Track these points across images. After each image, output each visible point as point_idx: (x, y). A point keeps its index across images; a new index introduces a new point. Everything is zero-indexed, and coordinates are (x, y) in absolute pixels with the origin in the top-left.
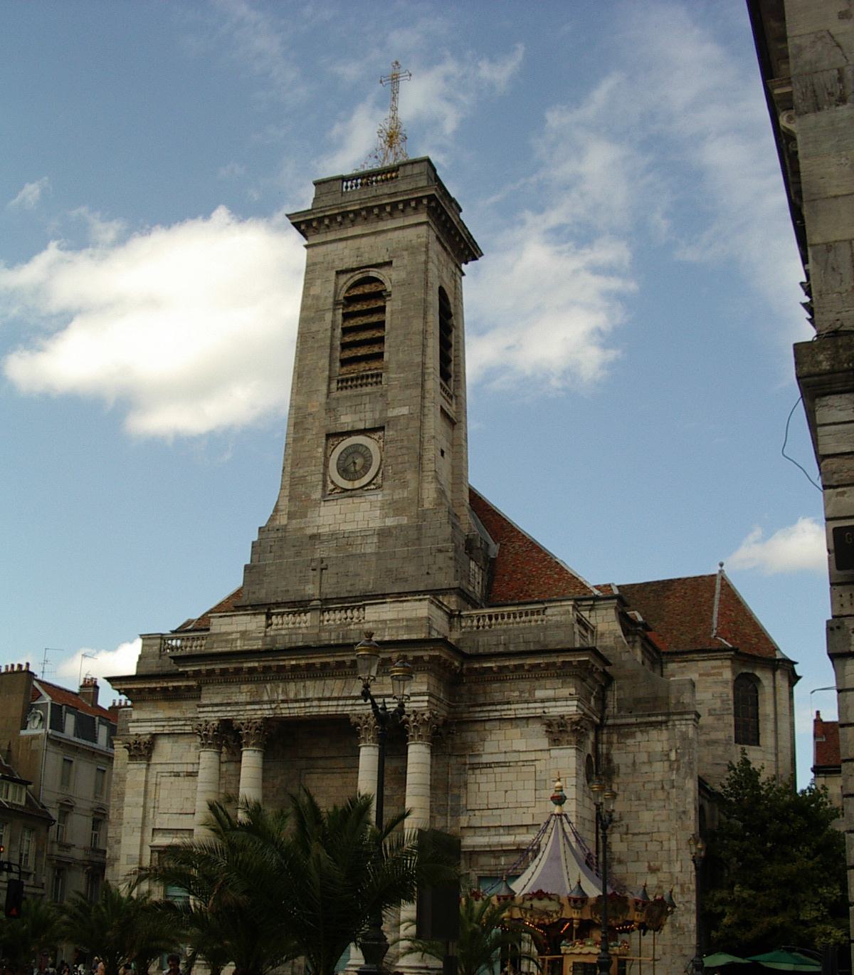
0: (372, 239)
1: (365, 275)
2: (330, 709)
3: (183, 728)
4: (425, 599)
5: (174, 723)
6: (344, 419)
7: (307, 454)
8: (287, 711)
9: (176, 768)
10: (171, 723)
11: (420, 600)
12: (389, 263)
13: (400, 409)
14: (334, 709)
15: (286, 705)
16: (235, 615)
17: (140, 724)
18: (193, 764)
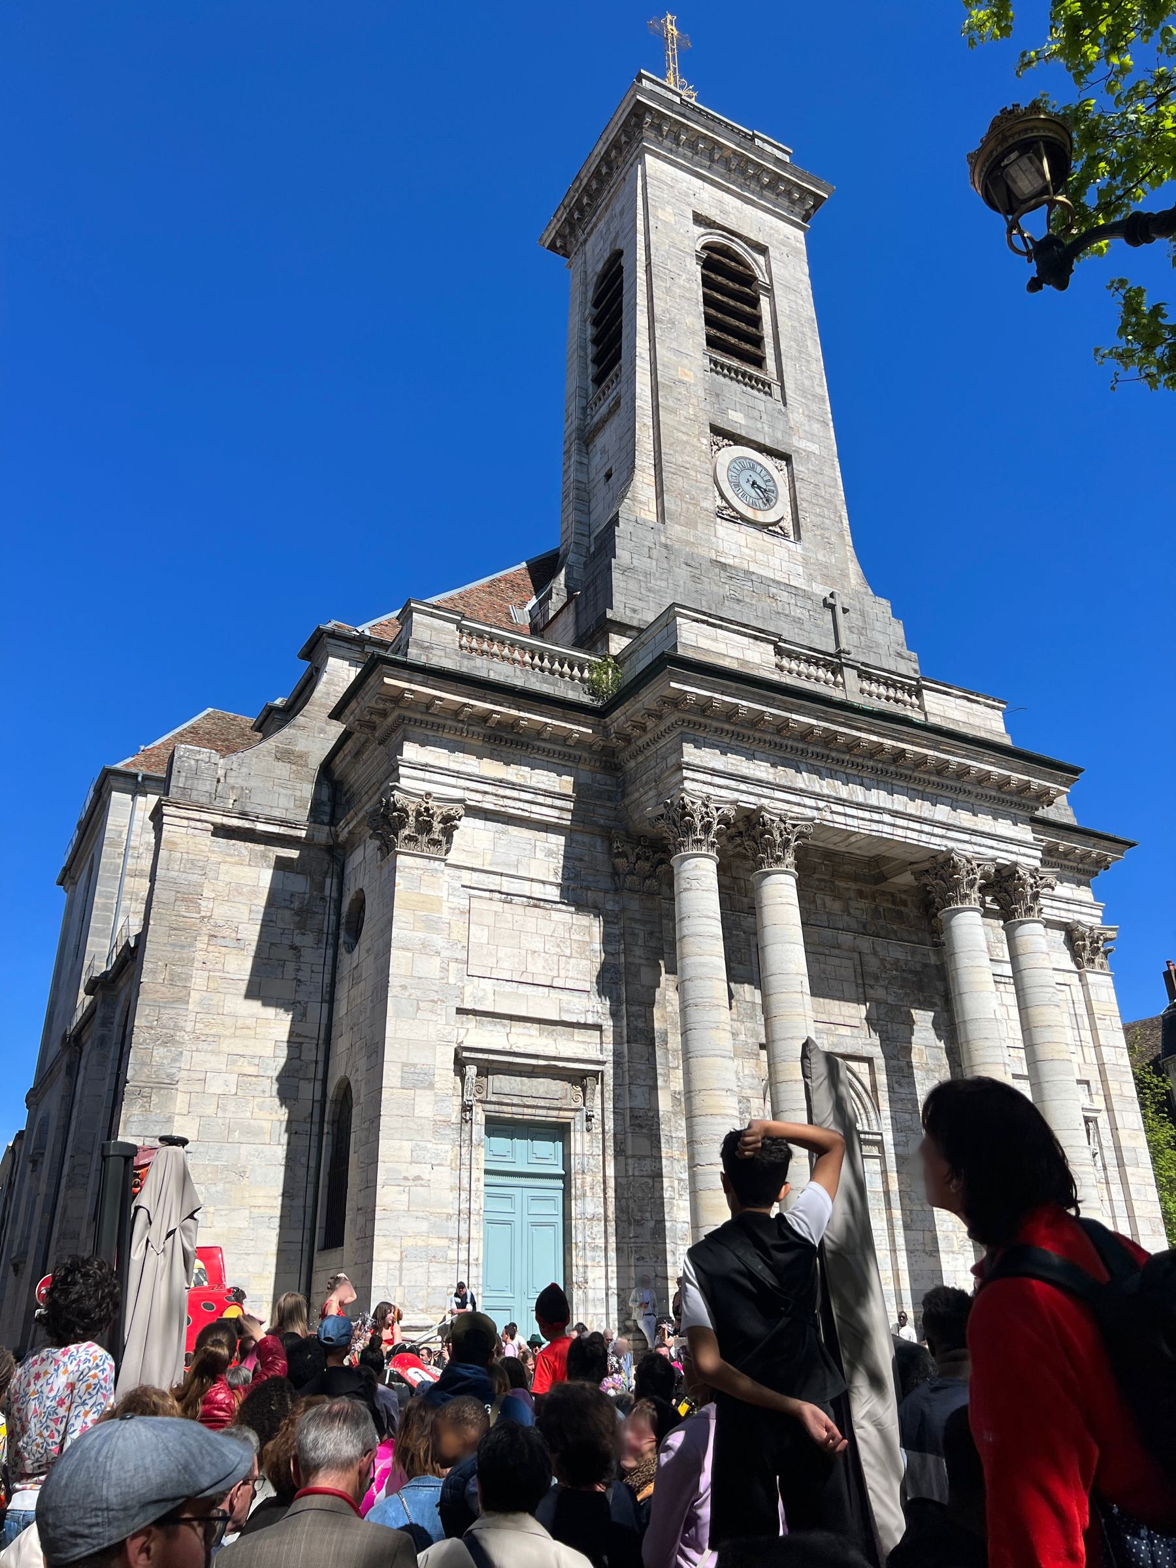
0: (738, 203)
2: (910, 834)
3: (526, 806)
4: (998, 709)
5: (508, 793)
6: (733, 415)
7: (685, 438)
8: (841, 819)
9: (508, 885)
10: (501, 792)
11: (993, 707)
13: (809, 444)
14: (915, 835)
15: (840, 809)
16: (720, 627)
17: (428, 776)
18: (543, 882)
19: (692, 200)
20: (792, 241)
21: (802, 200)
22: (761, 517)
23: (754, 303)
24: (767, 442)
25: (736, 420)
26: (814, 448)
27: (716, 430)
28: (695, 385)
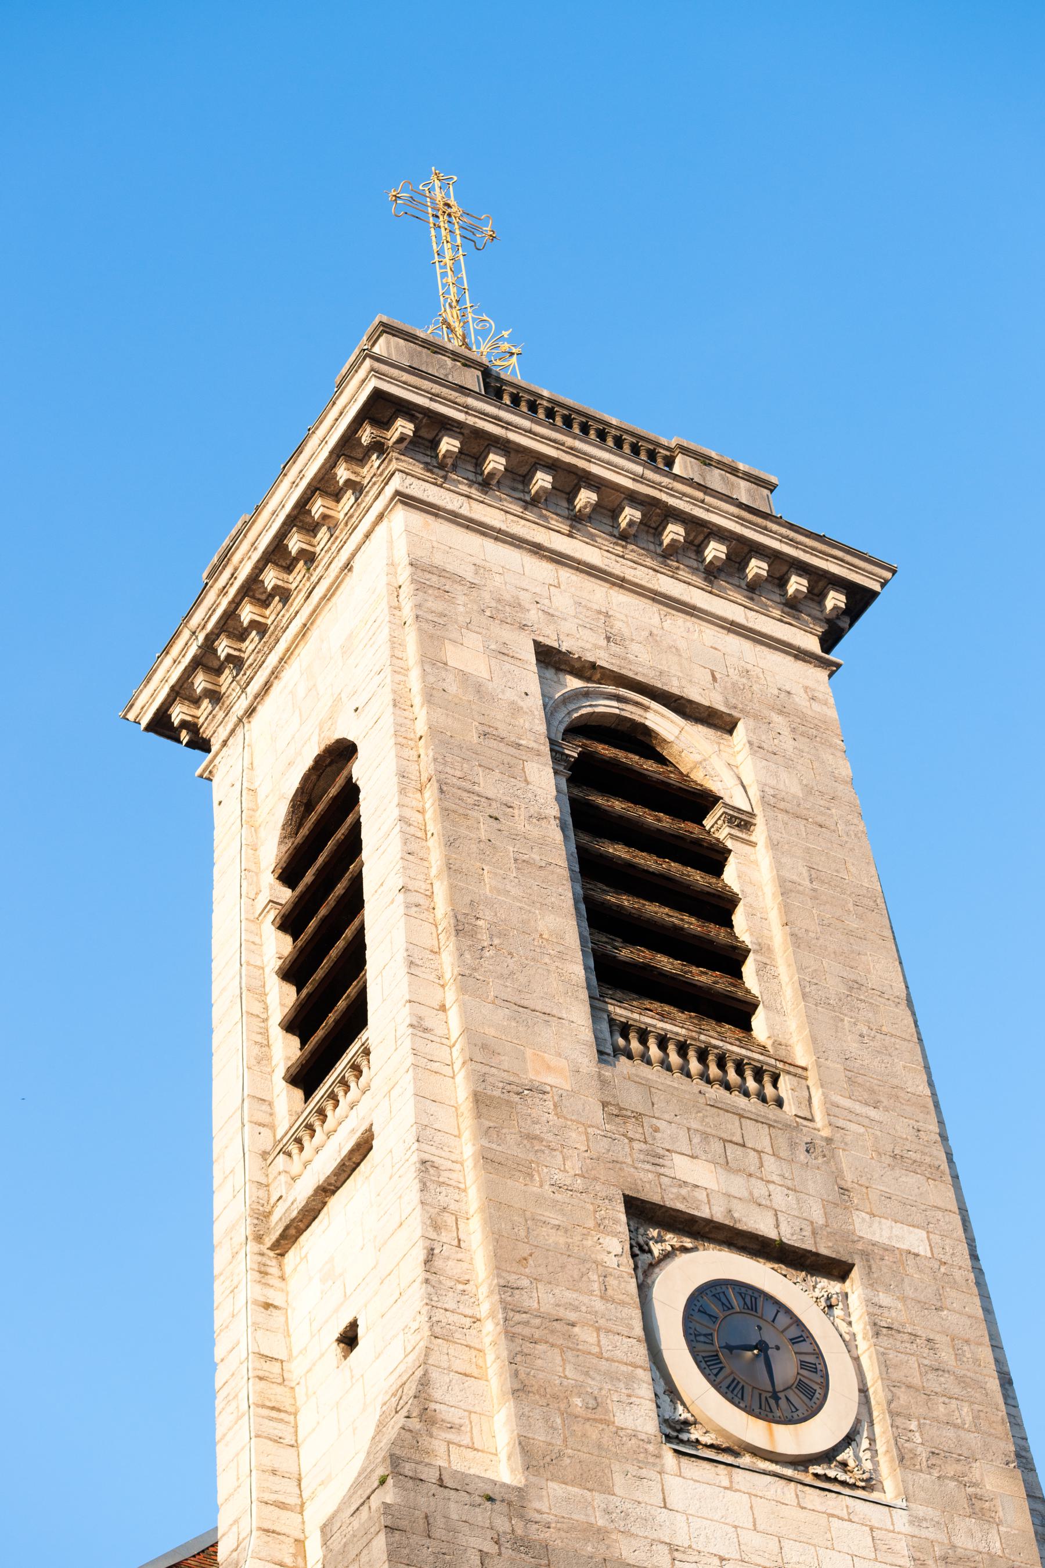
0: (650, 613)
1: (630, 712)
6: (682, 1167)
12: (720, 722)
13: (899, 1229)
19: (533, 616)
20: (801, 700)
21: (816, 595)
22: (791, 1439)
23: (714, 859)
24: (789, 1234)
25: (698, 1181)
26: (915, 1240)
27: (642, 1212)
28: (573, 1093)
